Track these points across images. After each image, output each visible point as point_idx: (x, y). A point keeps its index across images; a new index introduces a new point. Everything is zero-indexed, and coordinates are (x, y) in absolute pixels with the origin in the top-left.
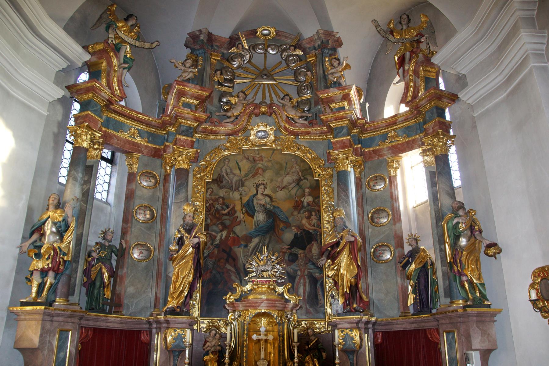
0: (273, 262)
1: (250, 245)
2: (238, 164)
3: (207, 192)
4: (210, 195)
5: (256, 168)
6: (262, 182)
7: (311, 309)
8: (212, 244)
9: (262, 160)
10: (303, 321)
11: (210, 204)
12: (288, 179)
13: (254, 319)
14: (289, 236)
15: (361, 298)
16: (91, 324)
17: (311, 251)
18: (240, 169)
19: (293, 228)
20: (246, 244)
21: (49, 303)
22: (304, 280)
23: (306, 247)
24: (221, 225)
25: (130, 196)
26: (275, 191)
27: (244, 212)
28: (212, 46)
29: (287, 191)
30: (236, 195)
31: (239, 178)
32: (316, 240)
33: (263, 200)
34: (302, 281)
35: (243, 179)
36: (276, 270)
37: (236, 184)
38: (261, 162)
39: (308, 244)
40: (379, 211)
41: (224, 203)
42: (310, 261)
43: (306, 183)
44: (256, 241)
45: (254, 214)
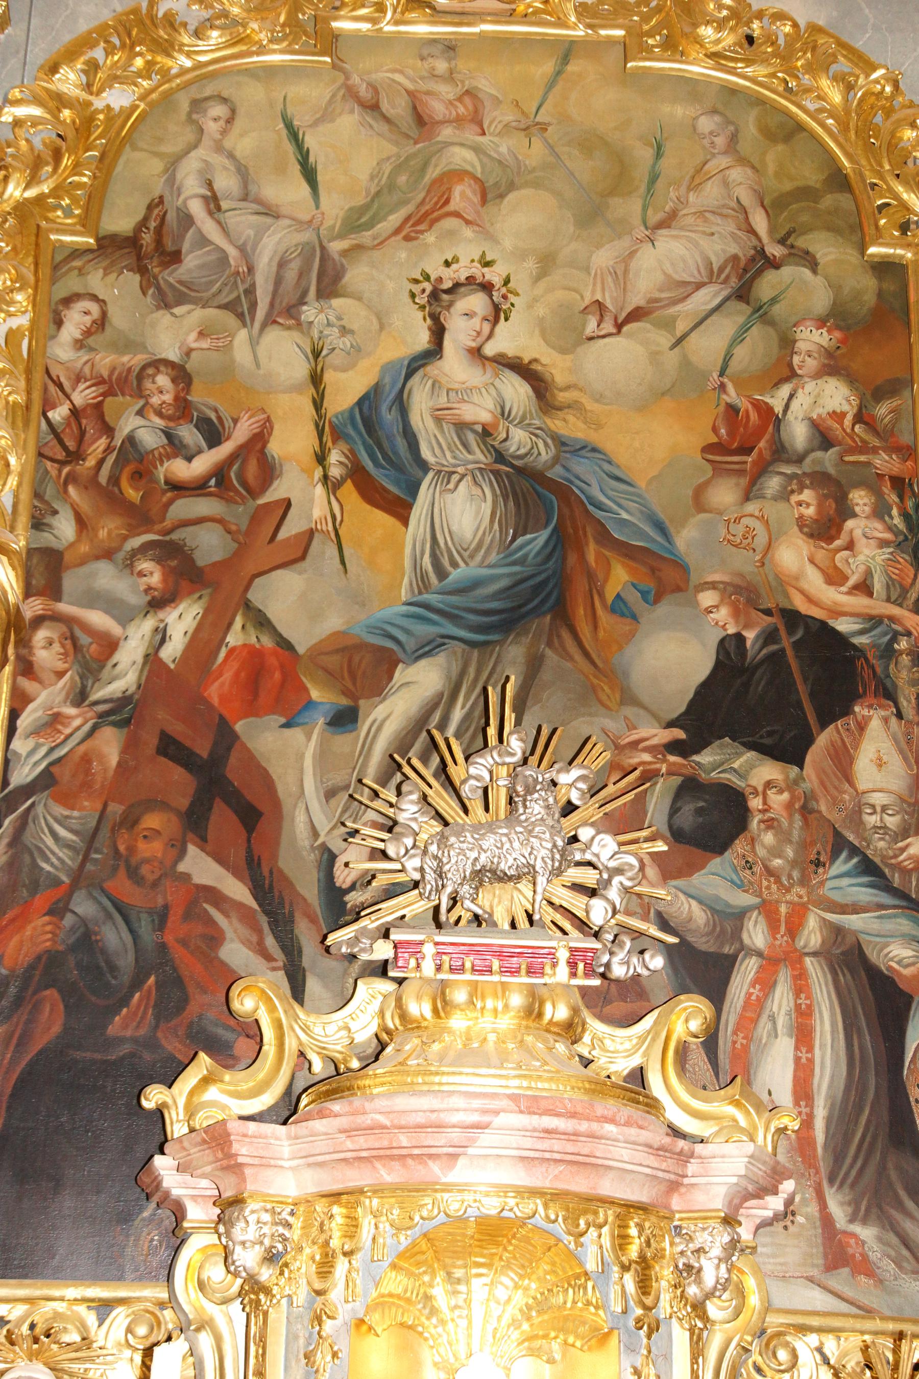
0: (569, 808)
1: (380, 712)
2: (294, 135)
3: (59, 323)
4: (79, 344)
5: (432, 173)
6: (477, 270)
7: (867, 1233)
8: (80, 697)
9: (477, 120)
10: (803, 1329)
11: (75, 412)
13: (394, 1283)
17: (848, 776)
18: (310, 175)
19: (707, 598)
20: (344, 702)
22: (800, 986)
23: (809, 741)
24: (159, 561)
27: (335, 472)
29: (664, 340)
31: (307, 236)
32: (888, 694)
35: (336, 247)
36: (589, 877)
37: (278, 281)
38: (470, 135)
39: (823, 726)
42: (839, 845)
45: (413, 489)
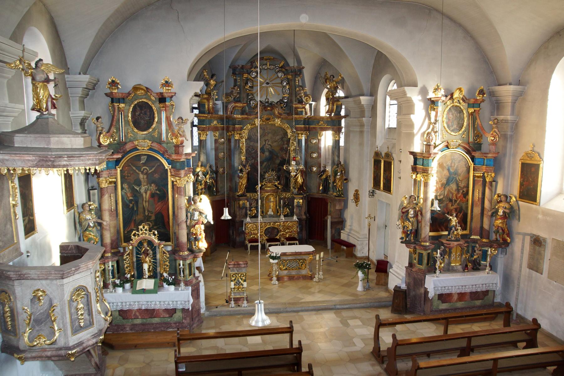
12: (278, 137)
14: (278, 161)
15: (304, 189)
28: (243, 70)
33: (268, 147)
34: (282, 179)
41: (252, 148)
43: (285, 139)
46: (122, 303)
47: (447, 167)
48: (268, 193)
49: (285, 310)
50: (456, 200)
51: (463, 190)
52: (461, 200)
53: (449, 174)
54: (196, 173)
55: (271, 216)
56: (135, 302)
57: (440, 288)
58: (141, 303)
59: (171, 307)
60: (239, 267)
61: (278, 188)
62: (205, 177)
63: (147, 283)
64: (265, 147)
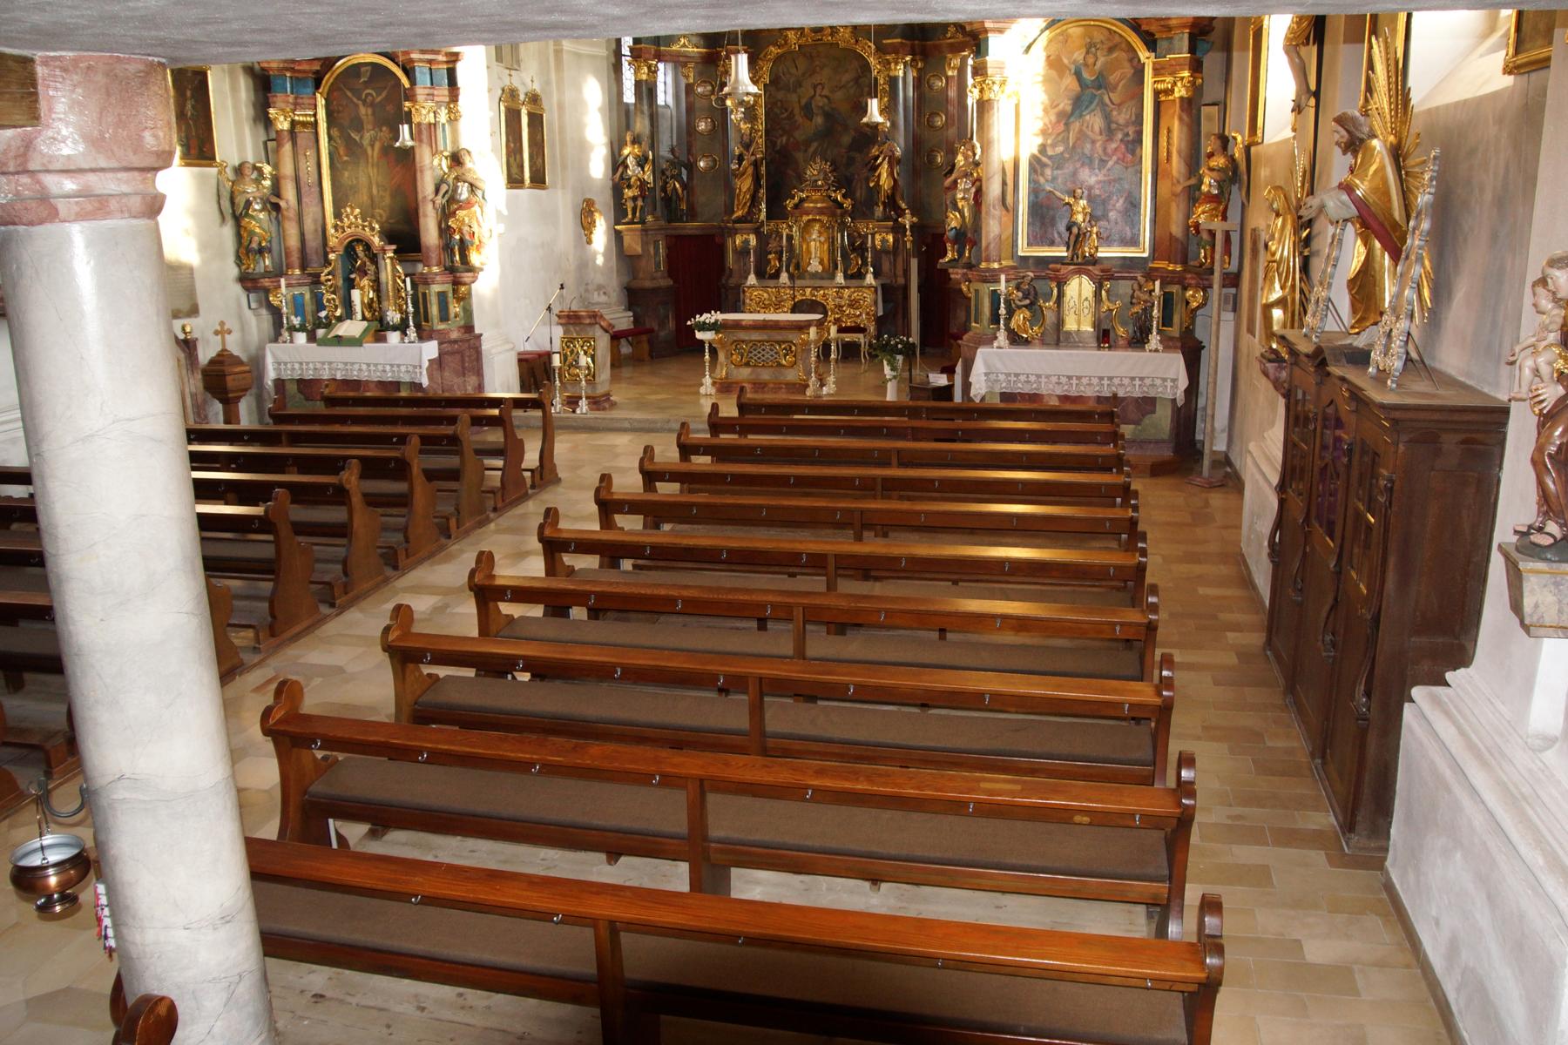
12: (846, 77)
14: (846, 140)
16: (673, 232)
21: (642, 222)
25: (690, 109)
26: (832, 91)
30: (794, 98)
34: (859, 185)
40: (934, 114)
44: (815, 145)
46: (301, 363)
47: (1073, 68)
48: (808, 214)
49: (666, 426)
50: (1104, 158)
51: (1126, 130)
52: (1119, 159)
53: (1081, 86)
54: (622, 158)
55: (815, 276)
56: (323, 363)
57: (1002, 377)
58: (334, 365)
59: (389, 377)
60: (581, 324)
61: (840, 205)
62: (643, 169)
63: (352, 328)
64: (813, 102)
